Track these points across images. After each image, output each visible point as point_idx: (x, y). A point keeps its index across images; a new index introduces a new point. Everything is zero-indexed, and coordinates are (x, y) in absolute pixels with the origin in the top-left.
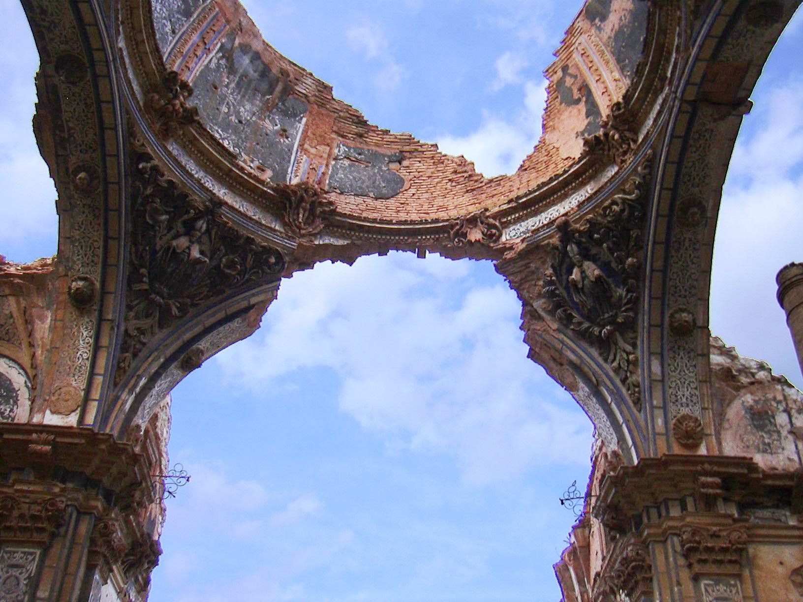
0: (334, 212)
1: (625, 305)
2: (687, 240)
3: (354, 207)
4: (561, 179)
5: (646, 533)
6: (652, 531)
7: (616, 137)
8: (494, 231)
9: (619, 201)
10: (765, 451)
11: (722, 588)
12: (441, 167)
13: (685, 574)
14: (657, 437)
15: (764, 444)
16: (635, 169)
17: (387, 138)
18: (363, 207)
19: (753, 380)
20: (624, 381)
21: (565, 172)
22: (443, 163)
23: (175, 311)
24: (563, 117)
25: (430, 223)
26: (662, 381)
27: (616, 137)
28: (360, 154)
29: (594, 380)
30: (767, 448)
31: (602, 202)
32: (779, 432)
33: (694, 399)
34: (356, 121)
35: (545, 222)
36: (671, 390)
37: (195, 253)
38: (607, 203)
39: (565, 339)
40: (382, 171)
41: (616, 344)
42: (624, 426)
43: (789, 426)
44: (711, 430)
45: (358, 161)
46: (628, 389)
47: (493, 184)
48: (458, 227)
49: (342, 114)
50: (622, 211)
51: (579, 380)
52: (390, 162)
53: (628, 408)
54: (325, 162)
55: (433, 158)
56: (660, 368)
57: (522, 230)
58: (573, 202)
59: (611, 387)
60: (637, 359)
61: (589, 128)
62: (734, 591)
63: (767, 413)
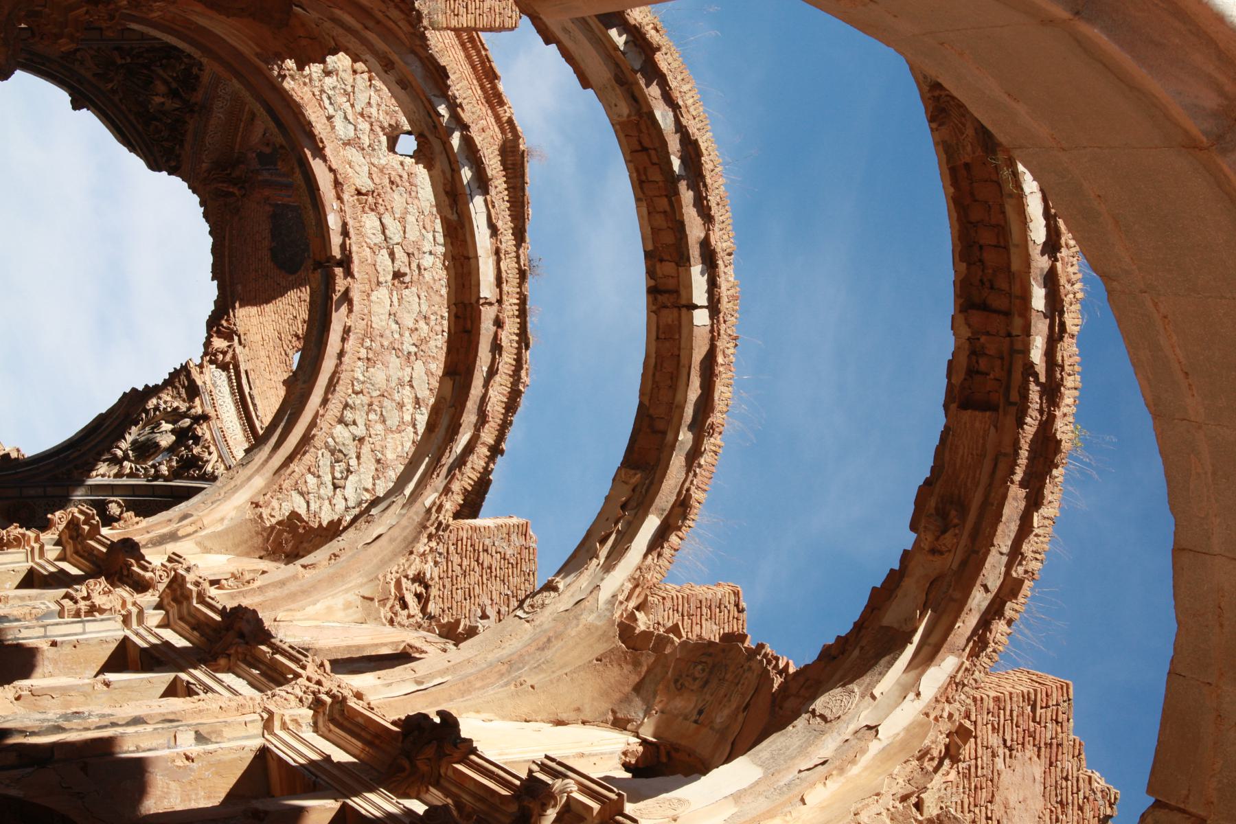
23: (111, 85)
38: (212, 448)
57: (219, 382)
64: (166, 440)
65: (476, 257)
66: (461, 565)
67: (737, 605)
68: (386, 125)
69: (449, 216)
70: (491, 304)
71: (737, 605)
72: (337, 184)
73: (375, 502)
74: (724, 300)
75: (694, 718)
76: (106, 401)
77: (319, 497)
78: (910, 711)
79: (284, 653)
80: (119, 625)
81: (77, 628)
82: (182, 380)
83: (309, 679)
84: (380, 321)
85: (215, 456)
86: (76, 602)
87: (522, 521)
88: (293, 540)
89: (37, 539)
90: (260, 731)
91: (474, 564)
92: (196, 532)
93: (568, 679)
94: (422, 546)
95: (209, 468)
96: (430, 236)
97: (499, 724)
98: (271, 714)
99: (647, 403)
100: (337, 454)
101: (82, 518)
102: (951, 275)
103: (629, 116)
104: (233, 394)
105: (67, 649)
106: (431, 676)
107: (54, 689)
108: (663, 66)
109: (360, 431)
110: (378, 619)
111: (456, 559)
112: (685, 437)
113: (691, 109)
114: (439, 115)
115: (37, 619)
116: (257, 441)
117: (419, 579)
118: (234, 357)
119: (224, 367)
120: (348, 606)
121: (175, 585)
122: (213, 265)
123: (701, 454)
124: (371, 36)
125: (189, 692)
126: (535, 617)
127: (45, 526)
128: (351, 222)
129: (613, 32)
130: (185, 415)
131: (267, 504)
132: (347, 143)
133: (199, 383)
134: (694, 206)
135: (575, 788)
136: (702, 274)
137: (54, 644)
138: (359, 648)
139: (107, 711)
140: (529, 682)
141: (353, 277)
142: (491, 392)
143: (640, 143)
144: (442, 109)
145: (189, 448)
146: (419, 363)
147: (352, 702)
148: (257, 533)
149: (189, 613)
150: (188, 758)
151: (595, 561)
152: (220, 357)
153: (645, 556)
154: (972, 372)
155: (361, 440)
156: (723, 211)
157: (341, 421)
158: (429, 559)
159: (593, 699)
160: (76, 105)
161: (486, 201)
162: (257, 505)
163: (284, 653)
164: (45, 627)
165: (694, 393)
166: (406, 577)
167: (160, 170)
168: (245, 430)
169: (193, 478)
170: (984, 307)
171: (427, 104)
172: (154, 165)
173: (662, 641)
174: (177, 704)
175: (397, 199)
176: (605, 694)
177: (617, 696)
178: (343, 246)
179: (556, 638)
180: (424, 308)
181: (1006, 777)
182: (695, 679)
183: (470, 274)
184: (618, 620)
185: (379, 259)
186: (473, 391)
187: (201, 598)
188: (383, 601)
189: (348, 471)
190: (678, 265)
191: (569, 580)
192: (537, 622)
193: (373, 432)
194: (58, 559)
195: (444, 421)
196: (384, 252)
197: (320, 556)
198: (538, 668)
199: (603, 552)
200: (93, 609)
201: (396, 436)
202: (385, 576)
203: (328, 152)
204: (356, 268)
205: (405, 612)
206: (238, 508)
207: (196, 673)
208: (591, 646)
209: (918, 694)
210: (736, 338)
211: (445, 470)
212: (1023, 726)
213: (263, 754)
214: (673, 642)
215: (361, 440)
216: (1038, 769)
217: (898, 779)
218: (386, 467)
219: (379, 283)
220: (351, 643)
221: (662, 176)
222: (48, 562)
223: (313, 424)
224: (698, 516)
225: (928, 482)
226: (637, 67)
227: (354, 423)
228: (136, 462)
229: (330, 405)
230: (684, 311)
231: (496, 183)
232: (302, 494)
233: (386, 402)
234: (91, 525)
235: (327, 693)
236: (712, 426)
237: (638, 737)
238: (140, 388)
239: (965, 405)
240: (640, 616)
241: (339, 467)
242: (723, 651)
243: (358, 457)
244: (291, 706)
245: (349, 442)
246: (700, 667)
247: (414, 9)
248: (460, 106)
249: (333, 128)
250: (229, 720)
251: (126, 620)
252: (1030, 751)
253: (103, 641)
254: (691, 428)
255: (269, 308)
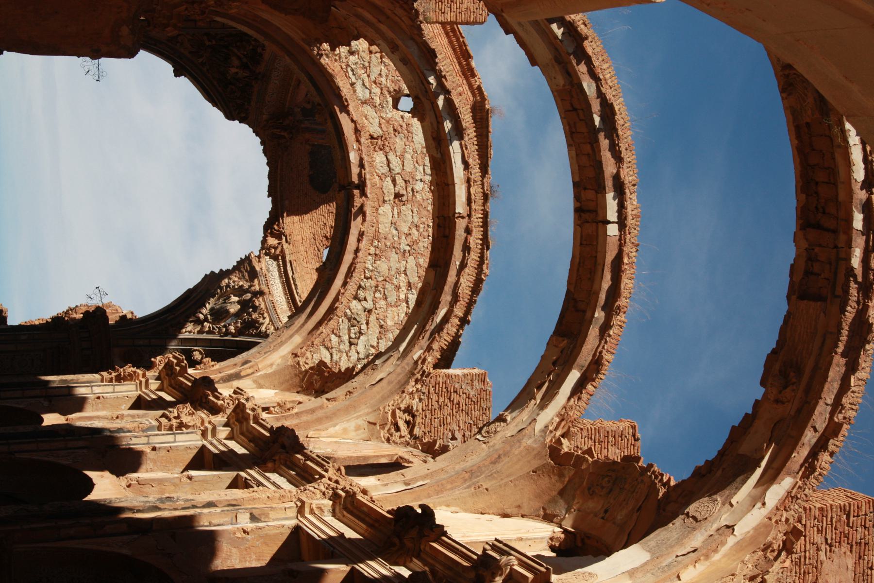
37: (233, 70)
38: (266, 315)
57: (271, 269)
64: (234, 308)
65: (454, 184)
66: (438, 402)
67: (634, 435)
68: (392, 90)
69: (435, 155)
70: (463, 217)
71: (634, 435)
72: (357, 131)
73: (379, 355)
74: (630, 218)
75: (601, 515)
76: (193, 280)
77: (340, 351)
78: (757, 515)
79: (313, 460)
80: (199, 437)
81: (170, 438)
82: (245, 266)
83: (330, 479)
84: (385, 228)
85: (267, 320)
86: (170, 420)
87: (482, 371)
88: (320, 381)
89: (144, 376)
90: (295, 514)
91: (447, 401)
92: (253, 373)
93: (512, 484)
94: (410, 388)
95: (263, 329)
96: (421, 168)
97: (463, 515)
98: (303, 503)
99: (572, 290)
100: (352, 320)
101: (175, 361)
102: (793, 203)
103: (564, 86)
104: (281, 277)
105: (163, 453)
106: (416, 480)
107: (153, 480)
108: (589, 51)
109: (369, 305)
110: (378, 438)
111: (434, 397)
112: (599, 314)
113: (609, 81)
114: (430, 83)
115: (143, 431)
116: (297, 310)
117: (408, 410)
118: (282, 251)
119: (275, 258)
120: (358, 428)
121: (238, 410)
122: (269, 186)
123: (610, 327)
124: (383, 28)
125: (246, 485)
126: (490, 440)
127: (150, 366)
128: (366, 158)
129: (554, 26)
130: (247, 291)
131: (303, 355)
132: (364, 102)
133: (258, 269)
134: (610, 150)
135: (516, 562)
136: (614, 199)
137: (154, 449)
138: (365, 458)
139: (190, 497)
140: (485, 486)
141: (366, 196)
142: (462, 279)
143: (572, 105)
144: (432, 80)
145: (250, 315)
146: (411, 258)
147: (360, 497)
148: (296, 375)
149: (248, 430)
150: (245, 532)
151: (533, 401)
152: (273, 251)
153: (569, 399)
154: (808, 273)
155: (370, 311)
156: (630, 154)
157: (356, 297)
158: (416, 396)
159: (530, 499)
160: (177, 74)
161: (461, 144)
162: (296, 355)
163: (313, 460)
164: (148, 436)
165: (606, 284)
166: (399, 409)
167: (234, 120)
168: (289, 303)
169: (252, 336)
170: (818, 227)
171: (421, 75)
172: (230, 116)
173: (580, 460)
174: (238, 494)
175: (399, 142)
176: (538, 496)
177: (547, 498)
178: (360, 175)
179: (505, 455)
180: (416, 219)
181: (827, 566)
182: (603, 487)
183: (449, 196)
184: (549, 444)
185: (385, 184)
186: (449, 279)
187: (256, 419)
188: (383, 426)
189: (361, 333)
190: (597, 192)
191: (514, 414)
192: (491, 444)
193: (378, 306)
194: (158, 390)
195: (428, 300)
196: (389, 179)
197: (339, 392)
198: (491, 476)
199: (539, 396)
200: (181, 425)
201: (394, 309)
202: (384, 408)
203: (351, 108)
204: (368, 191)
205: (398, 434)
206: (283, 357)
207: (252, 472)
208: (529, 462)
209: (764, 504)
210: (637, 245)
211: (428, 334)
212: (840, 529)
213: (297, 531)
214: (587, 460)
215: (370, 311)
216: (850, 561)
217: (748, 564)
218: (386, 331)
219: (384, 201)
220: (359, 454)
221: (587, 130)
222: (151, 391)
223: (336, 299)
224: (607, 372)
225: (774, 352)
226: (571, 50)
227: (365, 299)
228: (212, 323)
229: (348, 287)
230: (600, 225)
231: (469, 132)
232: (327, 348)
233: (388, 285)
234: (181, 367)
235: (342, 490)
236: (619, 307)
237: (561, 527)
238: (217, 271)
239: (802, 297)
240: (565, 441)
241: (353, 330)
242: (624, 468)
243: (367, 324)
244: (317, 498)
245: (361, 312)
246: (606, 479)
247: (413, 8)
248: (445, 77)
249: (355, 91)
250: (274, 506)
251: (204, 434)
252: (845, 548)
253: (188, 448)
254: (603, 309)
255: (307, 217)
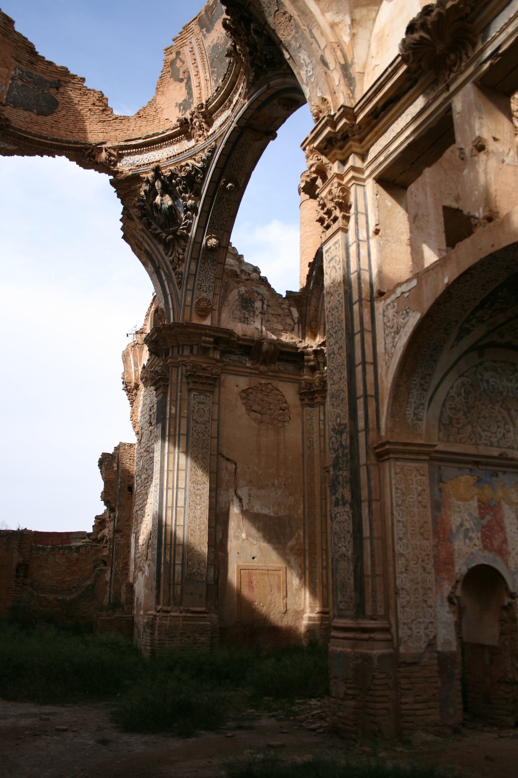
0: (9, 126)
1: (183, 225)
2: (225, 198)
3: (22, 119)
4: (160, 136)
5: (169, 361)
6: (173, 360)
7: (197, 124)
8: (113, 158)
9: (191, 165)
10: (244, 322)
11: (202, 397)
12: (85, 98)
13: (185, 388)
14: (186, 307)
15: (245, 317)
16: (203, 149)
17: (50, 68)
18: (28, 120)
19: (248, 278)
20: (174, 269)
21: (163, 133)
22: (86, 95)
24: (170, 88)
25: (73, 144)
26: (195, 275)
27: (197, 124)
28: (30, 78)
29: (157, 264)
30: (245, 320)
31: (181, 161)
32: (254, 312)
33: (211, 288)
34: (29, 51)
35: (146, 162)
36: (199, 282)
38: (183, 164)
39: (146, 237)
40: (44, 93)
41: (174, 246)
42: (169, 296)
43: (261, 309)
44: (216, 307)
45: (28, 82)
46: (176, 275)
47: (118, 121)
48: (90, 151)
49: (20, 44)
50: (191, 171)
51: (149, 262)
52: (51, 87)
53: (174, 286)
54: (4, 81)
55: (80, 90)
56: (195, 267)
57: (131, 162)
58: (165, 153)
59: (167, 271)
60: (184, 258)
61: (184, 105)
62: (208, 399)
63: (251, 299)
64: (168, 201)
82: (124, 186)
85: (190, 162)
92: (342, 51)
104: (141, 153)
118: (114, 148)
119: (120, 157)
130: (153, 186)
168: (172, 144)
169: (203, 179)
